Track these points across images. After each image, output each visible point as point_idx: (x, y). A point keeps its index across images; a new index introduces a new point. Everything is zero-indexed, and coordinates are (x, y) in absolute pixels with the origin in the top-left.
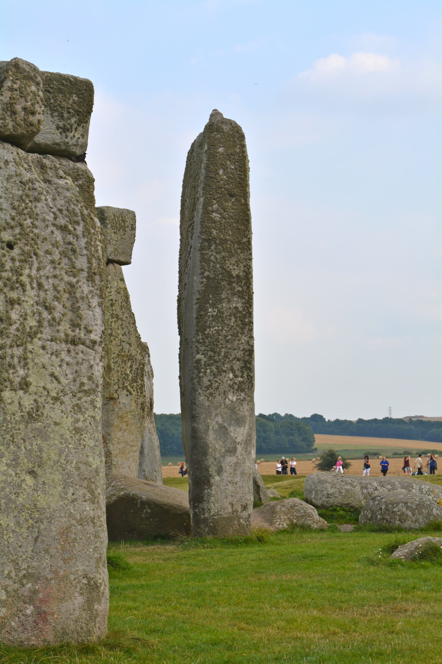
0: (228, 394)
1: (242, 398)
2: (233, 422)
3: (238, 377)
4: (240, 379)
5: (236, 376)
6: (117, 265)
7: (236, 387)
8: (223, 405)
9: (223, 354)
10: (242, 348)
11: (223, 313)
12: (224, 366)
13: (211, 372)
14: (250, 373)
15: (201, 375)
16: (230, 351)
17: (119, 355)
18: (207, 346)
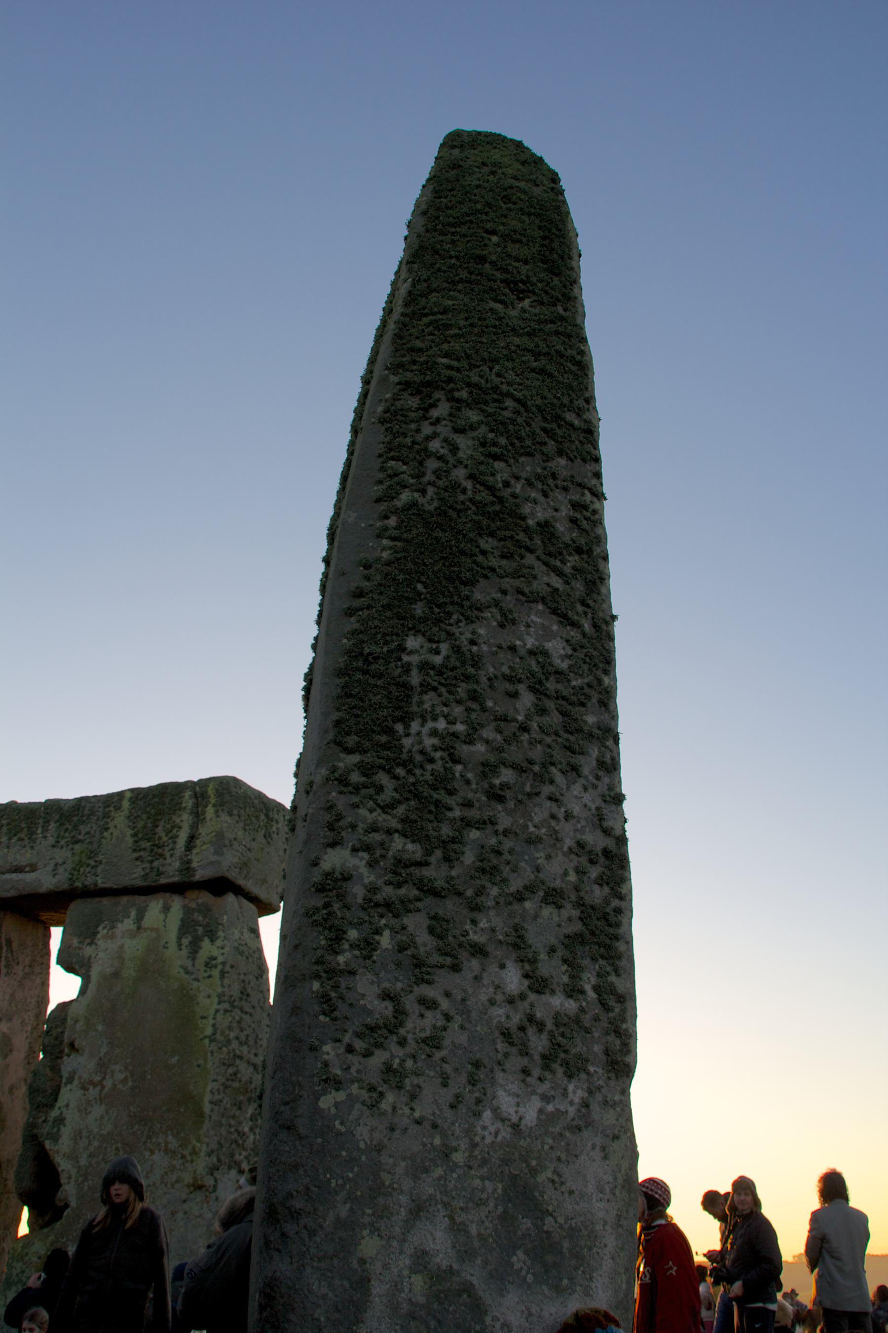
0: (494, 1083)
1: (572, 1110)
2: (519, 1259)
3: (553, 992)
4: (558, 1002)
5: (539, 985)
6: (252, 907)
7: (539, 1043)
8: (464, 1144)
9: (469, 858)
10: (569, 842)
11: (476, 662)
12: (474, 922)
13: (402, 948)
14: (612, 978)
15: (341, 959)
16: (508, 844)
17: (226, 1087)
18: (386, 808)
